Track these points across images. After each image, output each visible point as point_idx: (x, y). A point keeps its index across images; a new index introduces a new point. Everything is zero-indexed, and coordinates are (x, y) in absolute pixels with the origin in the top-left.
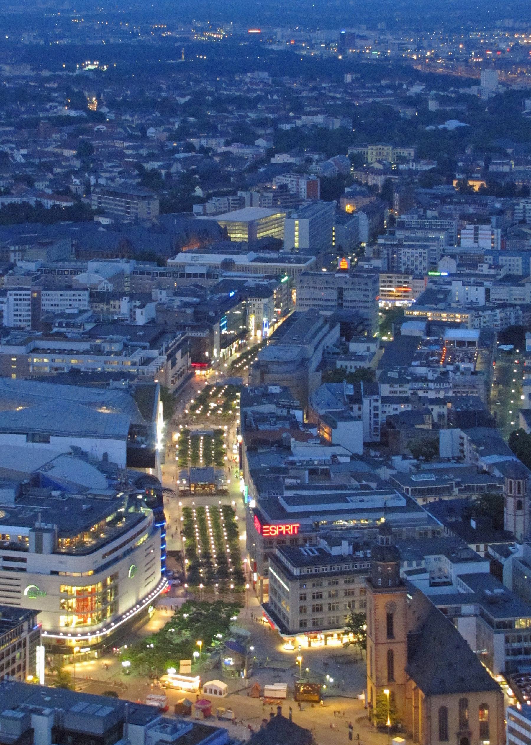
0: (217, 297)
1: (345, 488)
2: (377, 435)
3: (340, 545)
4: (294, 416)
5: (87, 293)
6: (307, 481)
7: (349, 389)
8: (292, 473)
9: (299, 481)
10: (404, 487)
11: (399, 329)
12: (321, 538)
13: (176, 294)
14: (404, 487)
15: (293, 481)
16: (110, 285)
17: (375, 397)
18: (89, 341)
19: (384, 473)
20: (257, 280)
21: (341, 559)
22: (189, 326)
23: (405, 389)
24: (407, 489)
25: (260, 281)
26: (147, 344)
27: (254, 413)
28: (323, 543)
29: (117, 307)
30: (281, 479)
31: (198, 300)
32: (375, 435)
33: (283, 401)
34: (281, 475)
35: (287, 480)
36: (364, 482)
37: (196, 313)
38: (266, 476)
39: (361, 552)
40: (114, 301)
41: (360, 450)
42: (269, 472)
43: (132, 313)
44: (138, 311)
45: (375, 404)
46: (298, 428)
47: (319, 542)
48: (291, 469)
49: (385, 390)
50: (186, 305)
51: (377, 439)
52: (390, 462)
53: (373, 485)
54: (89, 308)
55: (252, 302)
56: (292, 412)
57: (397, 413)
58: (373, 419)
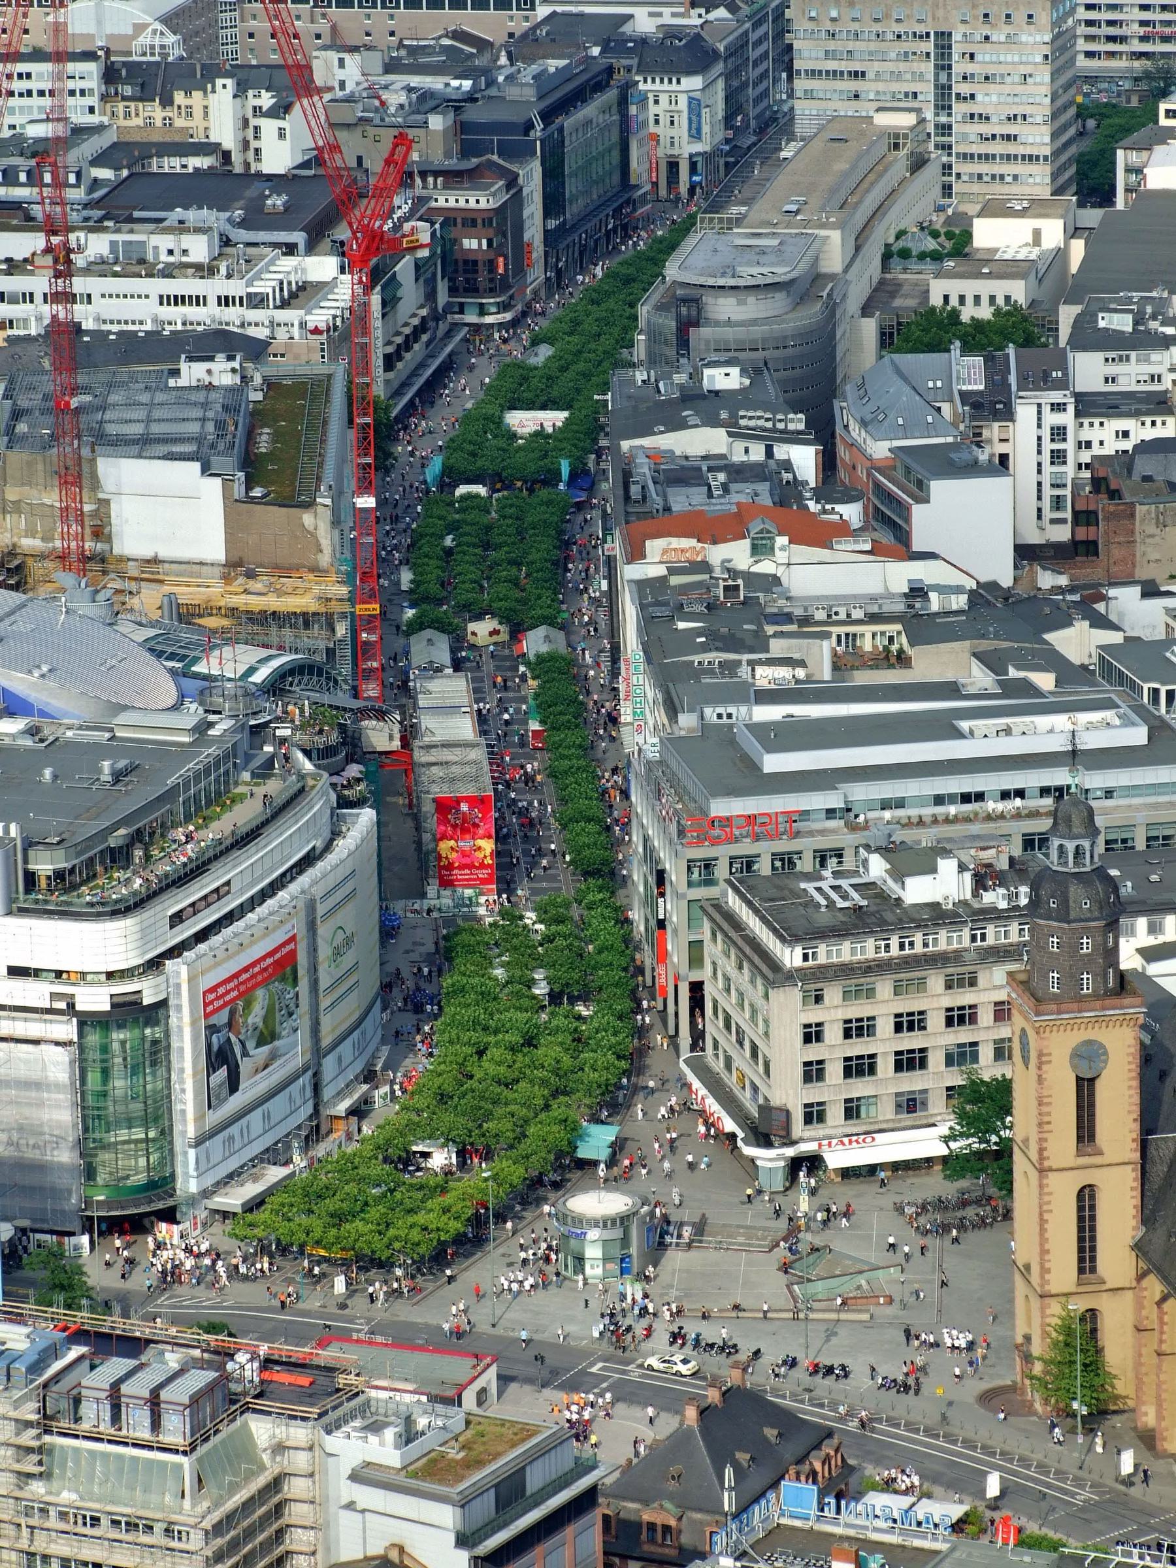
0: (528, 73)
1: (951, 690)
2: (1063, 521)
3: (933, 870)
4: (787, 465)
5: (91, 69)
6: (827, 675)
7: (969, 371)
8: (777, 647)
9: (801, 673)
10: (1146, 686)
11: (1139, 171)
12: (867, 847)
13: (391, 67)
14: (1146, 686)
15: (783, 673)
16: (171, 39)
17: (1057, 396)
18: (105, 230)
19: (1077, 642)
20: (667, 11)
21: (936, 916)
22: (436, 174)
23: (1155, 370)
24: (1156, 692)
25: (674, 15)
26: (298, 237)
27: (655, 456)
28: (877, 867)
29: (198, 112)
30: (744, 672)
31: (467, 84)
32: (1053, 521)
33: (751, 419)
34: (745, 657)
35: (760, 671)
36: (1013, 673)
37: (462, 127)
38: (697, 658)
39: (1002, 891)
40: (188, 93)
41: (1003, 573)
42: (704, 648)
43: (250, 133)
44: (269, 126)
45: (1052, 419)
46: (800, 498)
47: (865, 862)
48: (775, 635)
49: (1090, 370)
50: (426, 101)
51: (1062, 534)
52: (1100, 607)
53: (1045, 681)
54: (105, 120)
55: (649, 86)
56: (782, 451)
57: (1127, 445)
58: (1047, 468)
